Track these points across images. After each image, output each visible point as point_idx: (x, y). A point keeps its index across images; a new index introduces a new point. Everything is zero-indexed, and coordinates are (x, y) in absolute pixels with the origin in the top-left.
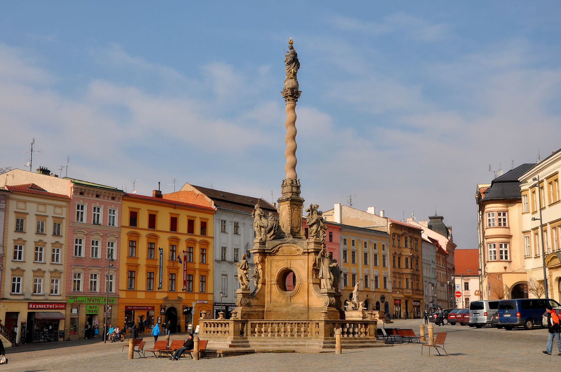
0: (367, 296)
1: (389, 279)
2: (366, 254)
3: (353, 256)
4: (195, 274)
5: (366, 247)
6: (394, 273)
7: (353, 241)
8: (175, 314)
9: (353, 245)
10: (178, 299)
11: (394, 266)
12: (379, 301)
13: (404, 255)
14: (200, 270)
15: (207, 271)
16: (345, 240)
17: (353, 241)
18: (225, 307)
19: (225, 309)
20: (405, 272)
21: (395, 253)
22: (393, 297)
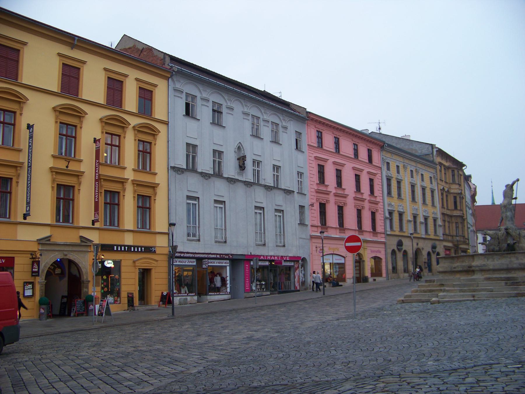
0: (417, 244)
1: (439, 222)
2: (413, 186)
3: (399, 188)
4: (124, 190)
5: (412, 176)
6: (443, 214)
7: (398, 167)
8: (78, 275)
9: (398, 172)
10: (79, 242)
11: (443, 207)
12: (431, 251)
13: (452, 193)
14: (137, 184)
15: (154, 187)
16: (388, 164)
17: (398, 167)
18: (195, 260)
19: (195, 264)
20: (454, 214)
21: (443, 189)
22: (445, 246)
